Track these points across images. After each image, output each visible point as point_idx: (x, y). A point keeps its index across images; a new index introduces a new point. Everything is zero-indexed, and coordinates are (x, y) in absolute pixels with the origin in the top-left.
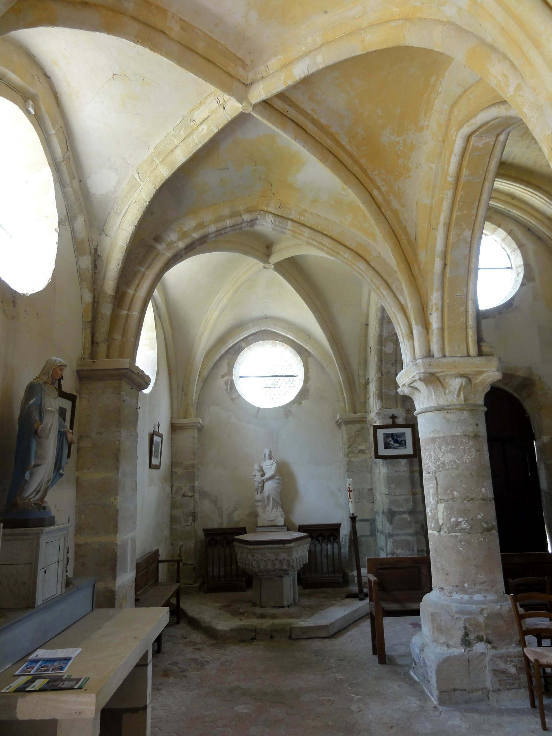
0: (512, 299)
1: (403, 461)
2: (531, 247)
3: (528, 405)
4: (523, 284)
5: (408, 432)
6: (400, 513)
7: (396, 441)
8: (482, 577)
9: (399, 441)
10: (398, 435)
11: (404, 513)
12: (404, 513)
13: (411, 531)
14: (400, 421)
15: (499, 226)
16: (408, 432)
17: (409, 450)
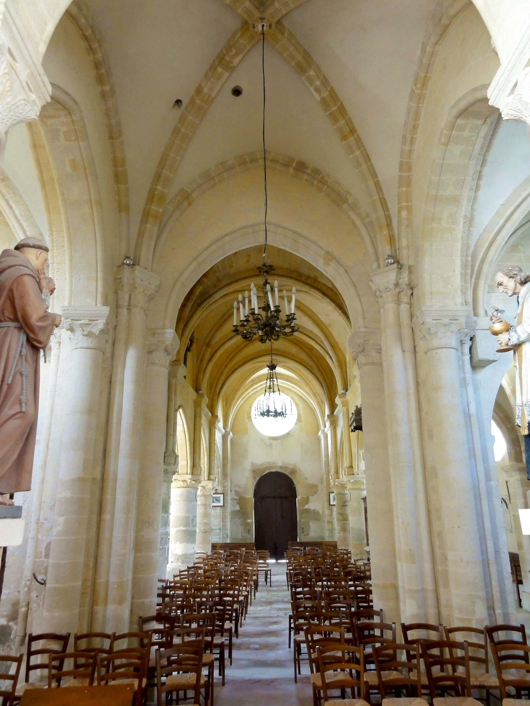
0: (290, 431)
1: (219, 508)
2: (301, 405)
3: (295, 481)
4: (296, 424)
5: (222, 496)
6: (215, 529)
7: (216, 500)
8: (200, 546)
9: (218, 500)
10: (217, 497)
11: (217, 529)
12: (217, 529)
13: (219, 537)
14: (219, 492)
15: (287, 395)
16: (222, 496)
17: (221, 504)
